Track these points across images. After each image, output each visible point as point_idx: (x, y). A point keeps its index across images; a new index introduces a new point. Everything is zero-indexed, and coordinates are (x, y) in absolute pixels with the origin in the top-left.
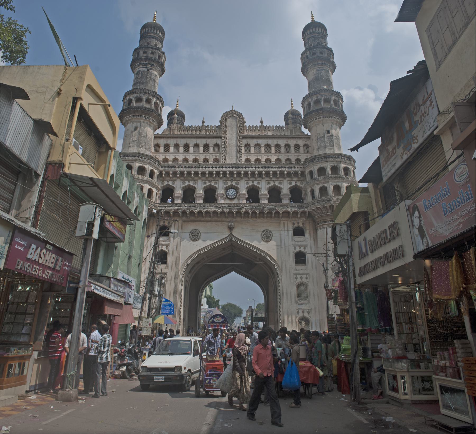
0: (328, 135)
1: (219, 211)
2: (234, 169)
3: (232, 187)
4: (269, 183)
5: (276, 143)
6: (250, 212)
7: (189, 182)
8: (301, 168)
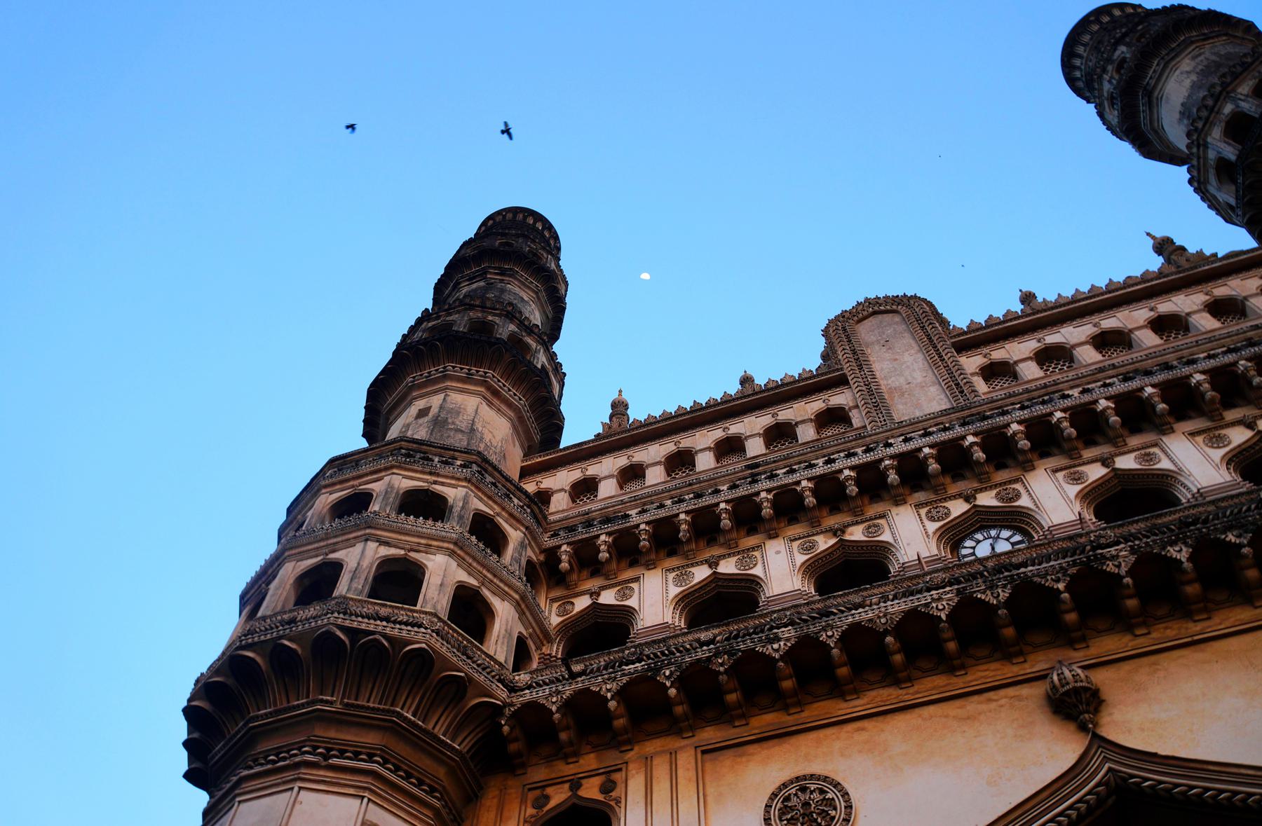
3: (981, 520)
6: (1180, 553)
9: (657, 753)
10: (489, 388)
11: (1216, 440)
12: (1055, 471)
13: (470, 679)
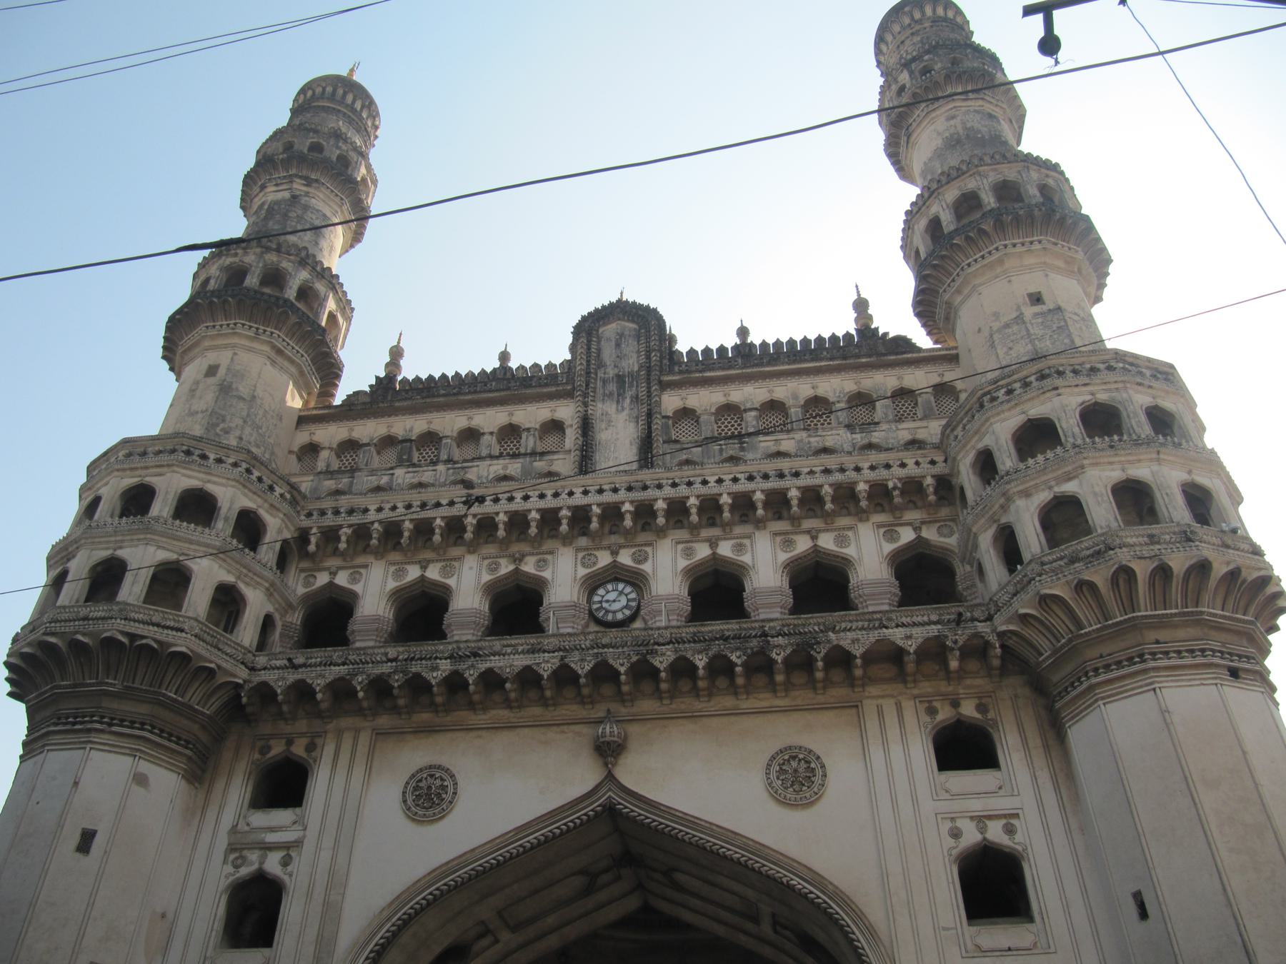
0: (1037, 309)
1: (546, 665)
2: (622, 495)
3: (615, 574)
4: (788, 544)
6: (701, 662)
7: (424, 568)
8: (933, 462)
10: (274, 347)
11: (788, 544)
12: (678, 543)
13: (219, 667)
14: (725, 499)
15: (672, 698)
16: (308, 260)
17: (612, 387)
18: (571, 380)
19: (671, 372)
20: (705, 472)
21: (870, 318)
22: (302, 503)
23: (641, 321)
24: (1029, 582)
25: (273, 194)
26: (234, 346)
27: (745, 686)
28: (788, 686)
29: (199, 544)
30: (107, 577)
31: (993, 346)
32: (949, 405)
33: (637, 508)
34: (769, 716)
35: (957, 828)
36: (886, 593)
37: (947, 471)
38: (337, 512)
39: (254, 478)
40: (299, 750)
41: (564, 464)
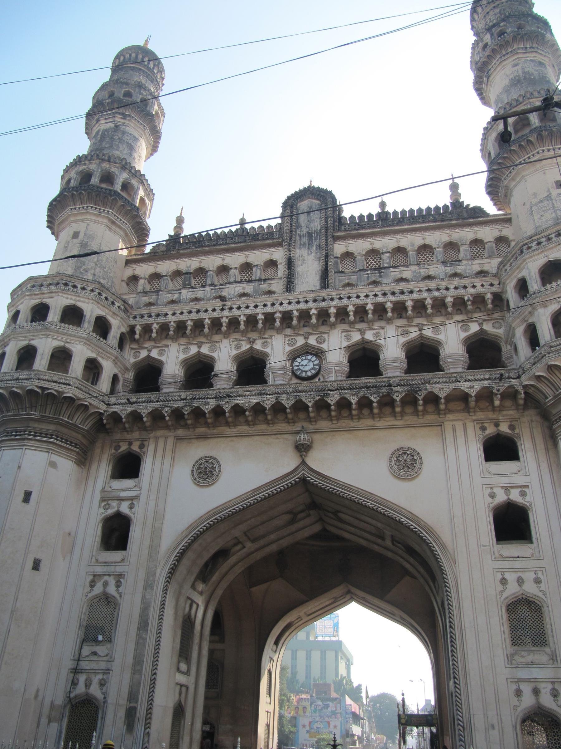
1: (268, 402)
2: (311, 304)
5: (421, 242)
6: (354, 400)
7: (200, 347)
8: (492, 285)
9: (161, 436)
10: (110, 220)
11: (406, 333)
12: (342, 332)
13: (90, 404)
14: (370, 307)
15: (338, 420)
16: (127, 166)
17: (305, 240)
18: (281, 236)
19: (339, 230)
20: (358, 291)
21: (459, 195)
22: (130, 311)
23: (322, 199)
24: (543, 357)
25: (104, 125)
26: (87, 220)
27: (378, 414)
28: (403, 414)
29: (75, 336)
30: (27, 356)
31: (531, 214)
32: (504, 248)
33: (319, 312)
34: (392, 431)
35: (493, 492)
36: (461, 361)
37: (500, 290)
38: (150, 316)
39: (103, 298)
40: (135, 447)
41: (277, 286)
